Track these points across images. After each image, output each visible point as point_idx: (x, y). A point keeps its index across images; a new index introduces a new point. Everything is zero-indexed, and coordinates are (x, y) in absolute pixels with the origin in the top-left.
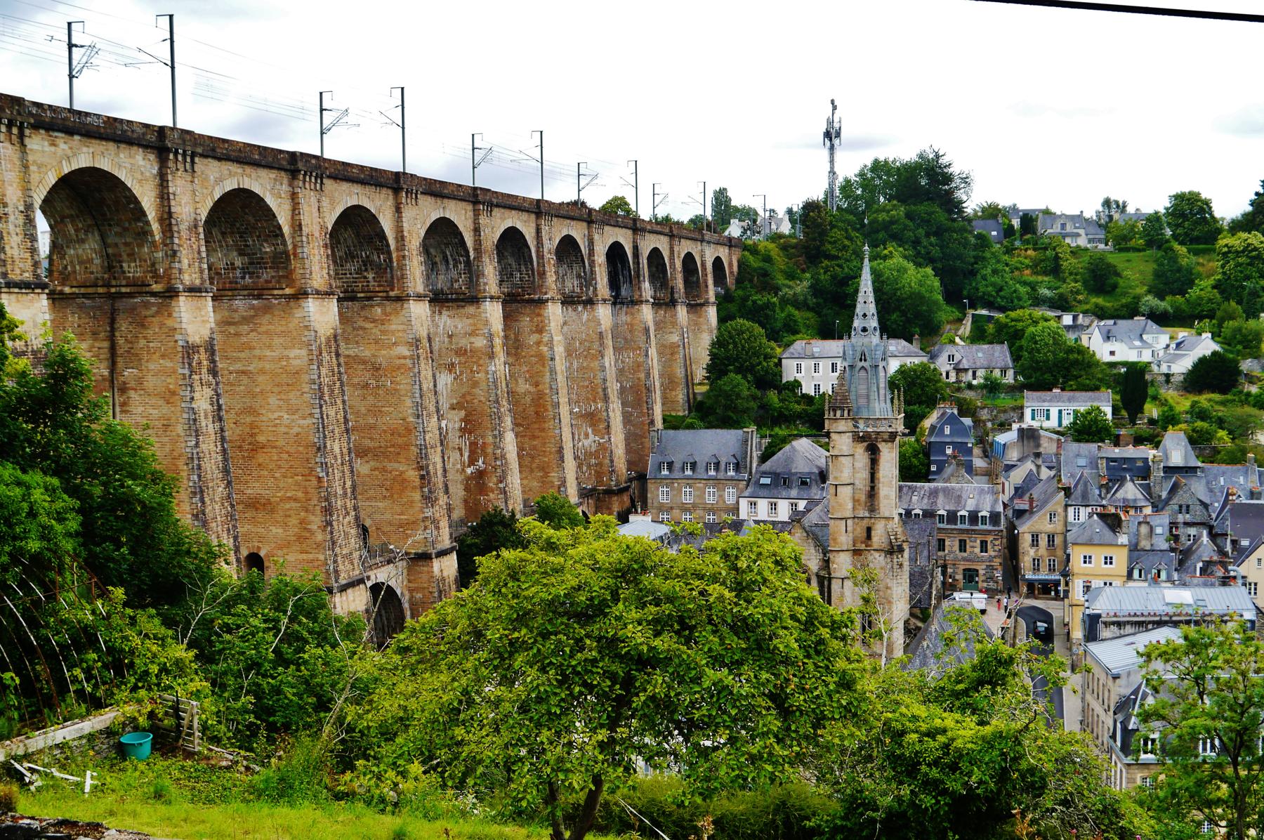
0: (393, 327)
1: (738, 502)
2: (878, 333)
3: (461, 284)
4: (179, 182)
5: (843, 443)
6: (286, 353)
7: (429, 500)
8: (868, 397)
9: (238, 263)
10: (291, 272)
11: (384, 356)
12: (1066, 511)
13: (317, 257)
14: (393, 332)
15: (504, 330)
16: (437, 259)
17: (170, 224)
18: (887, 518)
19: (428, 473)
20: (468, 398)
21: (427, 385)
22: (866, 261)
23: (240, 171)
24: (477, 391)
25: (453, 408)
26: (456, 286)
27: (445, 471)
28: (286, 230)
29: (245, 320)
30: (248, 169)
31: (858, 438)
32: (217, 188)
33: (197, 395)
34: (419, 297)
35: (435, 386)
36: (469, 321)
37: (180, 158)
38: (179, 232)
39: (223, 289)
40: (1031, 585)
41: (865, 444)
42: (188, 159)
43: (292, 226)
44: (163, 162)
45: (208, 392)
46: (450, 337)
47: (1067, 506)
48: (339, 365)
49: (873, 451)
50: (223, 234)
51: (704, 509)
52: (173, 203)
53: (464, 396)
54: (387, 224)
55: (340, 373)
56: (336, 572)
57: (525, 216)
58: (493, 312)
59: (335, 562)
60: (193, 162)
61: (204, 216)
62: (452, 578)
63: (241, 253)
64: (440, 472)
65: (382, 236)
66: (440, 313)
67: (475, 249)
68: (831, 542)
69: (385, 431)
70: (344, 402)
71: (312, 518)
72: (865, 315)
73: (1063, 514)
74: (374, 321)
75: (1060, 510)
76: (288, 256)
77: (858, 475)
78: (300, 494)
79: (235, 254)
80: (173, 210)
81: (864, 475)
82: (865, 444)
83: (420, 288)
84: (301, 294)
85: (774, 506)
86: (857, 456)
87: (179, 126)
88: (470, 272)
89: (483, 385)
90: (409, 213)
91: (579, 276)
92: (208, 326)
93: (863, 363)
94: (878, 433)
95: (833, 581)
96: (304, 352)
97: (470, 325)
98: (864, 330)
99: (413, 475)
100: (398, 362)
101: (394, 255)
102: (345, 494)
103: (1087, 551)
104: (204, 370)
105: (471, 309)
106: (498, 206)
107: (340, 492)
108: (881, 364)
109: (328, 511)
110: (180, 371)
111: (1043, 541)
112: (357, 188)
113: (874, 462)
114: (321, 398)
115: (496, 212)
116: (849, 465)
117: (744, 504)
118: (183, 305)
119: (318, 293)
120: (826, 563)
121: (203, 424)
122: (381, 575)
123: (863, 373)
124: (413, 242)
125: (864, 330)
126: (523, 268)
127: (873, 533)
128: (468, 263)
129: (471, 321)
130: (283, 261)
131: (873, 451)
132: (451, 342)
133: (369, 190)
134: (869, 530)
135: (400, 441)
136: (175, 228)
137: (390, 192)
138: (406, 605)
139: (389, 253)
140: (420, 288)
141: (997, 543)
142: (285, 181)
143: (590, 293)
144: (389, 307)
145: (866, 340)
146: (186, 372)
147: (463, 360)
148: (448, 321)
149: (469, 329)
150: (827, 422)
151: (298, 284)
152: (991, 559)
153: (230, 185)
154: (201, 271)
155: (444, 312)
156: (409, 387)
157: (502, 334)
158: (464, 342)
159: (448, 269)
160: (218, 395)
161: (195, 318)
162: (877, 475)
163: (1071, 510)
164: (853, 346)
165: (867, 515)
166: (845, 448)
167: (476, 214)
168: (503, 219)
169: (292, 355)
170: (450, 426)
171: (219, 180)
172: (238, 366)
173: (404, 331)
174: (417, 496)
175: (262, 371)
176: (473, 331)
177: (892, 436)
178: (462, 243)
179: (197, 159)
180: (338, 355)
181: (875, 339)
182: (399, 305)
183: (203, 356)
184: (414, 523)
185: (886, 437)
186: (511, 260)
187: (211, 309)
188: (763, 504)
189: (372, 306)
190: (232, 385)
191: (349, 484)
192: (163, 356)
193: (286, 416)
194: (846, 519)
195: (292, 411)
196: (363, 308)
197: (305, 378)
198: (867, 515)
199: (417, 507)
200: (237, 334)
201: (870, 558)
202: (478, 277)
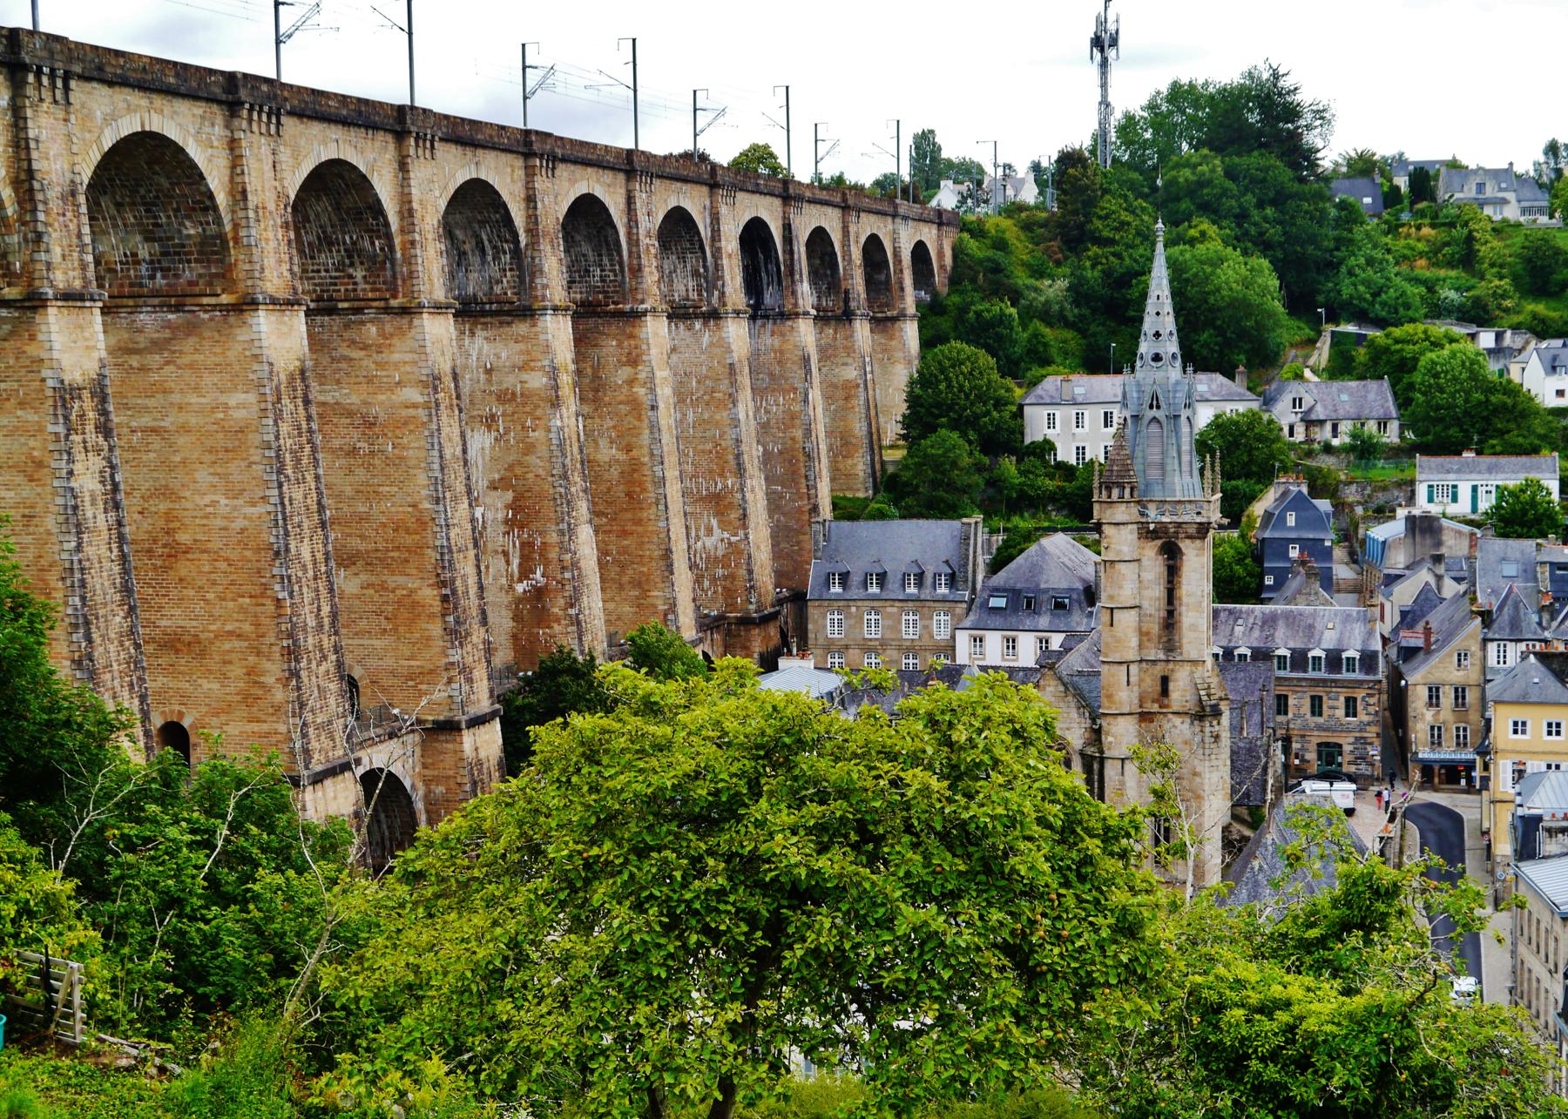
0: (396, 357)
1: (953, 638)
2: (1178, 363)
3: (506, 287)
4: (44, 120)
5: (1122, 540)
6: (223, 398)
7: (456, 635)
8: (1162, 466)
9: (143, 253)
10: (230, 268)
11: (381, 404)
12: (1484, 648)
13: (273, 244)
14: (396, 365)
15: (576, 362)
16: (467, 247)
17: (31, 190)
18: (1194, 662)
19: (454, 592)
20: (518, 471)
21: (452, 450)
22: (1160, 246)
23: (144, 102)
24: (532, 459)
25: (493, 486)
26: (497, 289)
27: (481, 588)
28: (221, 199)
29: (157, 346)
30: (158, 101)
31: (1148, 533)
32: (107, 132)
33: (78, 468)
34: (438, 308)
35: (465, 451)
37: (45, 80)
38: (45, 203)
39: (119, 295)
40: (1427, 769)
41: (1159, 542)
42: (59, 83)
43: (232, 193)
44: (17, 88)
45: (97, 462)
46: (489, 372)
47: (1485, 641)
48: (309, 418)
49: (1171, 553)
50: (119, 205)
51: (900, 648)
52: (34, 155)
53: (511, 467)
54: (384, 188)
55: (310, 431)
56: (307, 752)
57: (608, 176)
58: (558, 332)
59: (304, 735)
60: (67, 88)
61: (86, 175)
62: (494, 762)
63: (149, 238)
64: (473, 590)
65: (377, 209)
66: (473, 334)
67: (528, 231)
68: (1104, 701)
69: (384, 525)
70: (317, 477)
71: (268, 665)
72: (1157, 335)
73: (1479, 654)
74: (365, 347)
75: (1475, 648)
76: (224, 242)
77: (1147, 593)
78: (247, 628)
79: (138, 238)
80: (35, 166)
81: (1157, 592)
82: (1159, 542)
83: (440, 294)
84: (247, 304)
85: (1011, 644)
86: (1145, 562)
87: (43, 28)
88: (520, 268)
89: (542, 450)
90: (420, 172)
91: (696, 274)
92: (96, 355)
93: (1154, 412)
95: (1108, 765)
96: (252, 398)
97: (521, 352)
98: (1157, 358)
99: (429, 595)
100: (405, 413)
101: (397, 241)
102: (320, 626)
103: (1519, 713)
104: (90, 427)
105: (521, 328)
106: (564, 160)
107: (311, 622)
108: (1184, 414)
109: (293, 653)
110: (51, 428)
111: (1448, 697)
112: (335, 132)
113: (1173, 572)
114: (279, 472)
115: (563, 170)
116: (1134, 578)
117: (963, 639)
118: (55, 324)
119: (274, 301)
120: (1096, 735)
121: (89, 514)
122: (378, 757)
123: (1154, 428)
124: (428, 219)
125: (1157, 358)
126: (606, 260)
127: (1171, 686)
128: (517, 253)
129: (521, 346)
130: (217, 249)
131: (1171, 553)
132: (489, 381)
133: (355, 135)
134: (1165, 681)
135: (409, 540)
136: (39, 196)
137: (389, 138)
138: (419, 806)
139: (389, 237)
140: (440, 294)
141: (1372, 701)
142: (219, 120)
143: (715, 301)
144: (390, 324)
145: (1160, 375)
146: (61, 429)
147: (509, 408)
148: (485, 347)
149: (519, 360)
150: (1096, 507)
151: (241, 286)
152: (1362, 727)
153: (129, 126)
154: (84, 267)
155: (480, 333)
156: (422, 454)
157: (572, 367)
158: (510, 381)
159: (484, 262)
160: (112, 467)
161: (74, 343)
162: (1177, 593)
163: (1492, 648)
164: (1138, 384)
165: (1162, 656)
166: (1125, 549)
167: (530, 173)
168: (572, 181)
169: (232, 403)
170: (489, 516)
171: (111, 118)
172: (146, 420)
173: (415, 363)
174: (436, 629)
175: (185, 429)
176: (526, 363)
177: (1203, 530)
178: (508, 220)
179: (73, 84)
180: (307, 402)
181: (1174, 373)
182: (405, 321)
183: (88, 403)
184: (431, 672)
185: (1192, 530)
186: (586, 248)
187: (99, 328)
188: (994, 640)
189: (363, 323)
190: (135, 450)
191: (326, 609)
192: (22, 404)
193: (223, 501)
194: (1128, 663)
195: (234, 493)
196: (347, 326)
197: (255, 439)
198: (1162, 656)
199: (436, 651)
200: (143, 369)
201: (1167, 726)
202: (533, 276)
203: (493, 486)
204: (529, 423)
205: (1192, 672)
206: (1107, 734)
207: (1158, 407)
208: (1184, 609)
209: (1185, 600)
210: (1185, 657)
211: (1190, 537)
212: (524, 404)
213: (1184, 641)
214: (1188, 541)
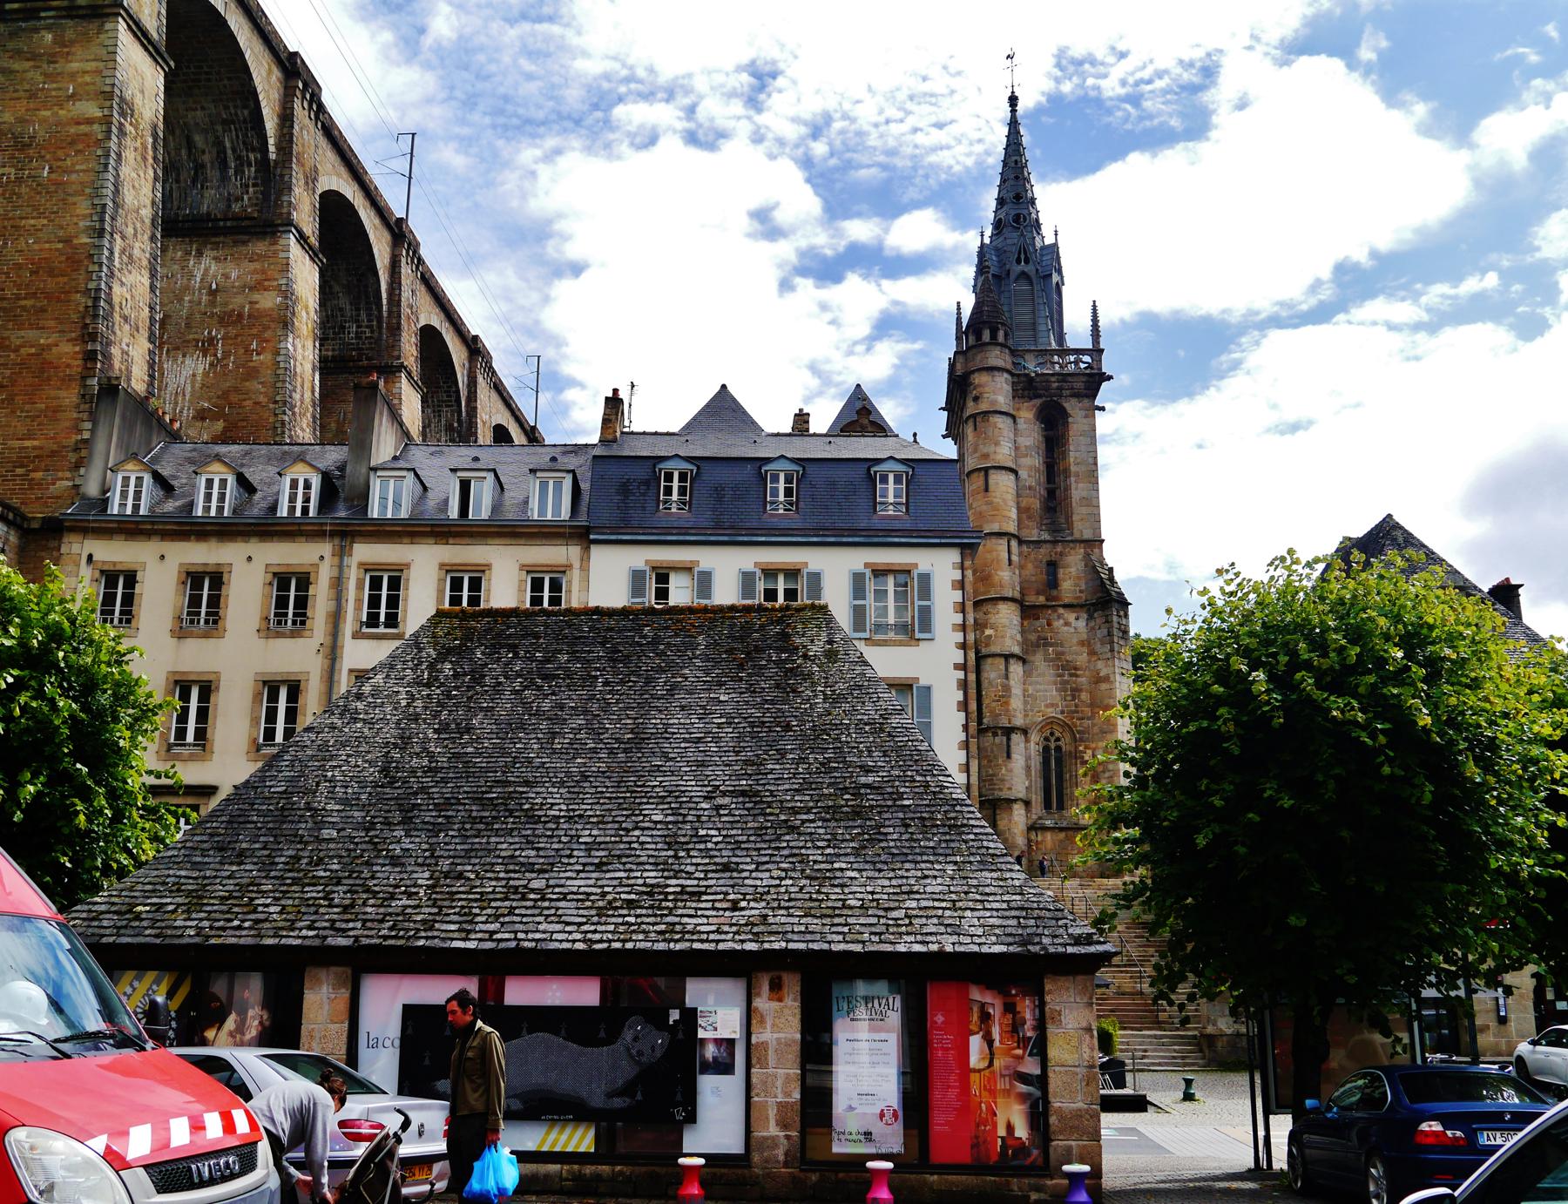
0: (75, 66)
3: (247, 203)
11: (44, 121)
14: (73, 76)
16: (206, 158)
20: (234, 398)
24: (254, 385)
26: (236, 207)
31: (1026, 387)
36: (252, 266)
46: (213, 293)
53: (225, 395)
66: (200, 254)
67: (279, 148)
69: (19, 267)
74: (34, 57)
82: (1038, 402)
94: (1063, 377)
97: (255, 272)
99: (67, 351)
105: (260, 247)
129: (257, 265)
132: (212, 303)
135: (51, 284)
144: (71, 29)
147: (233, 331)
156: (92, 176)
158: (237, 302)
159: (224, 178)
165: (1046, 536)
166: (1001, 399)
173: (98, 72)
174: (70, 396)
176: (259, 283)
182: (93, 26)
184: (53, 454)
185: (1079, 385)
186: (344, 302)
189: (36, 30)
196: (13, 35)
198: (1046, 536)
201: (1058, 624)
202: (280, 193)
203: (201, 416)
204: (254, 346)
205: (1087, 556)
209: (1073, 468)
210: (1077, 535)
212: (251, 326)
214: (1074, 401)
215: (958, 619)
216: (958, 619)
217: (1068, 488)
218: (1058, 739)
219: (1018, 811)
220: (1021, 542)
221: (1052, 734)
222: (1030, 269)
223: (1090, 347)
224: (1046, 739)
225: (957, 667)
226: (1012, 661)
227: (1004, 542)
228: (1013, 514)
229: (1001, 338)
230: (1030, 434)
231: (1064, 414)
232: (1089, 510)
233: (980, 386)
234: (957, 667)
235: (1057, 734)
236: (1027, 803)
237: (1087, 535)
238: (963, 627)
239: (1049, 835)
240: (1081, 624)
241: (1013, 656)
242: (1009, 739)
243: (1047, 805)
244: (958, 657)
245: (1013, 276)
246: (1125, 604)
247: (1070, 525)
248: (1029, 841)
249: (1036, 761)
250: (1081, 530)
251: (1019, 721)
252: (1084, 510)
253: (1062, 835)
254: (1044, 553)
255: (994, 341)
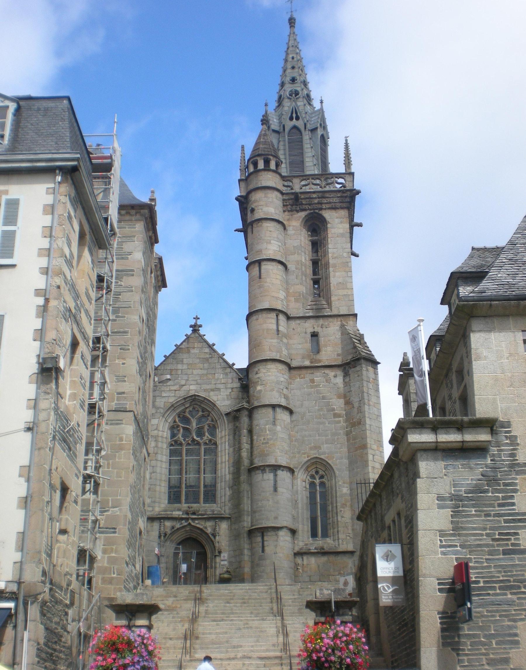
31: (294, 202)
41: (303, 214)
77: (295, 257)
82: (303, 214)
94: (323, 194)
113: (318, 245)
127: (322, 340)
205: (342, 326)
206: (256, 383)
207: (297, 118)
208: (331, 269)
209: (331, 261)
210: (335, 312)
211: (335, 208)
213: (333, 298)
215: (45, 243)
216: (45, 243)
217: (327, 277)
218: (322, 477)
219: (284, 537)
220: (289, 318)
221: (317, 472)
222: (300, 124)
223: (343, 171)
224: (312, 477)
225: (38, 293)
226: (278, 410)
227: (273, 315)
228: (282, 295)
229: (273, 166)
230: (299, 237)
231: (324, 221)
232: (345, 292)
233: (255, 201)
234: (38, 293)
235: (321, 472)
236: (293, 532)
237: (344, 311)
238: (48, 252)
239: (313, 560)
240: (339, 380)
241: (280, 406)
242: (276, 475)
243: (314, 534)
244: (41, 282)
245: (287, 130)
246: (375, 363)
247: (329, 304)
248: (296, 565)
249: (303, 496)
250: (339, 306)
251: (283, 461)
252: (341, 292)
253: (324, 559)
254: (309, 326)
255: (267, 168)
